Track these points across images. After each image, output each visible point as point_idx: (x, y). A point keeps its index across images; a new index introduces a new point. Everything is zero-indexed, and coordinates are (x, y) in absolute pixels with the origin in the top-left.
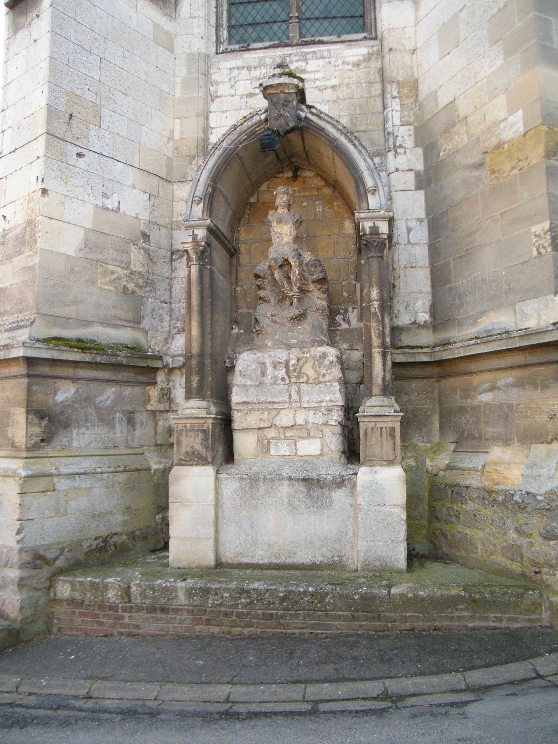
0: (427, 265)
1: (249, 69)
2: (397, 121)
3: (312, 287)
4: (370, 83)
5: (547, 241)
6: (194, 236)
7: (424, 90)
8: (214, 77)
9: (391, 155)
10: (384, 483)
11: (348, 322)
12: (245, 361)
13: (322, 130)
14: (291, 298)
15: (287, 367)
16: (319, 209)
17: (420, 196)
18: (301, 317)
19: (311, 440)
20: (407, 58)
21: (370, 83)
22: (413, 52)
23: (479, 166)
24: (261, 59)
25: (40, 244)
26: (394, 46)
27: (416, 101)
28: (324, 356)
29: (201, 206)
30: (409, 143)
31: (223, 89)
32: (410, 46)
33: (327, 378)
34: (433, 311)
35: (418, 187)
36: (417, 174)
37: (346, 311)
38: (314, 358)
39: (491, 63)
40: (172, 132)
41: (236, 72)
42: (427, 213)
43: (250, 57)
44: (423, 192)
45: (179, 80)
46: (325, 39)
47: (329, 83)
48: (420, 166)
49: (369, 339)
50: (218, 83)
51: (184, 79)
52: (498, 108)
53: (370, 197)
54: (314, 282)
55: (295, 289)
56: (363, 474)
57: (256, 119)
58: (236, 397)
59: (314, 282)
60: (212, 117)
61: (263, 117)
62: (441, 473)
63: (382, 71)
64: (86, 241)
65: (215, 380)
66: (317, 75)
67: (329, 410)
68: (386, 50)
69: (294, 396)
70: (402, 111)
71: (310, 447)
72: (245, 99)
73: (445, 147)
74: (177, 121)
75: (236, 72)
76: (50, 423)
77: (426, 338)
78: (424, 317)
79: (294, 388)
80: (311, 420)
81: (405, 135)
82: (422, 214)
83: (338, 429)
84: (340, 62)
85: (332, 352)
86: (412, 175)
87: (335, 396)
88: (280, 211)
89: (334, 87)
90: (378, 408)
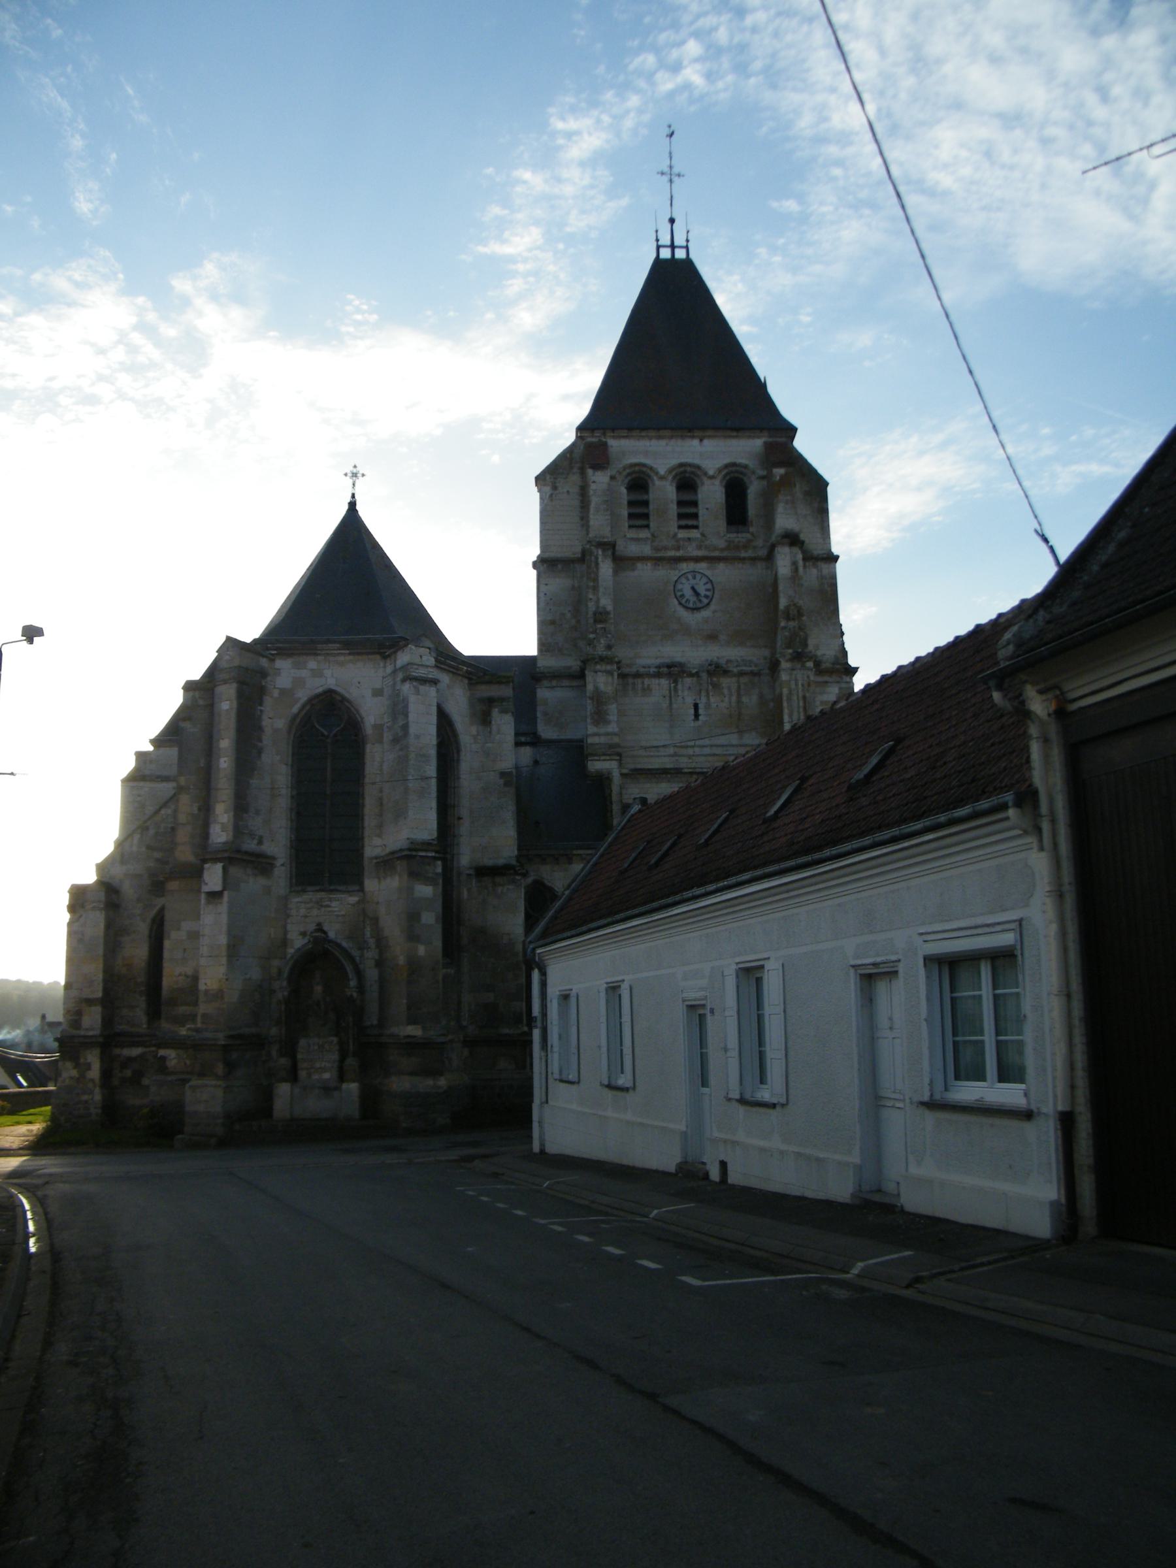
12: (303, 1042)
30: (373, 946)
43: (306, 897)
58: (299, 1056)
65: (289, 1049)
71: (327, 1076)
76: (230, 1066)
85: (335, 1039)
87: (335, 1056)
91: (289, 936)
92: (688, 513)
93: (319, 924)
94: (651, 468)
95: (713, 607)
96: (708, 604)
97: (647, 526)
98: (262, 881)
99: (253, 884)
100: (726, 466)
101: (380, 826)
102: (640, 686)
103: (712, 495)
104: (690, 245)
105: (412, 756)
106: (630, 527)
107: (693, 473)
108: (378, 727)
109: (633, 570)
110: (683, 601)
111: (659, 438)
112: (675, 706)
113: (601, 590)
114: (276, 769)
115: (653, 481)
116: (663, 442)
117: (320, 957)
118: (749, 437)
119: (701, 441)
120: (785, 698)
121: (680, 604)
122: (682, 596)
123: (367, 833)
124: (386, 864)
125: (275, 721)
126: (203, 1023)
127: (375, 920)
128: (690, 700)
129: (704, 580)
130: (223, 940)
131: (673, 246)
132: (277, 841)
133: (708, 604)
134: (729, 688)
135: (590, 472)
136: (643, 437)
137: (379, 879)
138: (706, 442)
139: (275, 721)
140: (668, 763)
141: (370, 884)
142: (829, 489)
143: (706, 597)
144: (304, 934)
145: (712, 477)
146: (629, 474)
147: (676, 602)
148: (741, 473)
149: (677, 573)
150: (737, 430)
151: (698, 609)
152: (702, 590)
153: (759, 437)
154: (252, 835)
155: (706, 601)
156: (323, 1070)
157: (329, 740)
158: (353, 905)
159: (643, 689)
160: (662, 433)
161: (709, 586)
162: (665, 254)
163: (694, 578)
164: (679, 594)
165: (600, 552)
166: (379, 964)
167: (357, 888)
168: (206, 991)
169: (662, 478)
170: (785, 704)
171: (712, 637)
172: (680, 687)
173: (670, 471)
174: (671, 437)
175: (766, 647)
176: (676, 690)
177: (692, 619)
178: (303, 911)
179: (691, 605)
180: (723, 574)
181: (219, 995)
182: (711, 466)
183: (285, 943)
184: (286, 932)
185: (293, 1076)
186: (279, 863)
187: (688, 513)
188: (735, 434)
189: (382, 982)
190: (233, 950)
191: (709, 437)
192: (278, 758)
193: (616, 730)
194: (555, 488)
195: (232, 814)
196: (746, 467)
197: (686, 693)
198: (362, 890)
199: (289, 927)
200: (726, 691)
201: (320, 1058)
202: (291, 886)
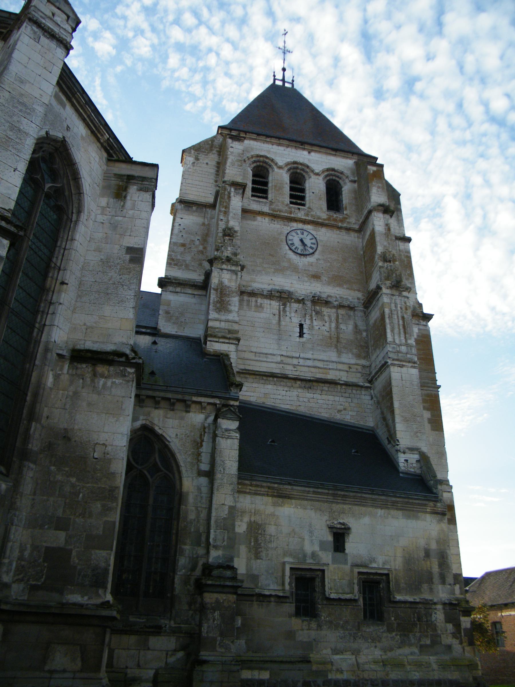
92: (298, 193)
94: (272, 160)
95: (316, 255)
96: (313, 253)
97: (266, 198)
100: (328, 170)
102: (253, 304)
103: (315, 187)
104: (294, 83)
106: (252, 196)
107: (303, 170)
109: (254, 220)
110: (293, 248)
111: (279, 145)
112: (283, 323)
113: (231, 215)
115: (273, 168)
116: (281, 148)
118: (344, 157)
119: (309, 153)
120: (387, 316)
121: (291, 249)
122: (293, 244)
128: (296, 321)
129: (310, 237)
131: (283, 80)
133: (313, 253)
134: (329, 316)
135: (229, 141)
136: (268, 142)
138: (313, 154)
140: (276, 369)
142: (401, 197)
143: (311, 248)
145: (317, 174)
146: (255, 162)
147: (287, 248)
148: (338, 177)
149: (289, 229)
150: (336, 150)
151: (305, 255)
152: (308, 242)
153: (351, 159)
155: (311, 251)
159: (256, 306)
160: (281, 141)
161: (314, 241)
162: (279, 83)
163: (303, 234)
164: (290, 242)
165: (233, 190)
169: (280, 168)
170: (387, 321)
171: (316, 277)
172: (288, 309)
173: (287, 164)
174: (288, 146)
175: (359, 291)
176: (284, 309)
177: (301, 262)
179: (299, 252)
180: (324, 235)
182: (318, 168)
187: (298, 193)
188: (334, 153)
191: (316, 151)
193: (237, 319)
194: (197, 159)
196: (342, 173)
197: (293, 314)
200: (326, 318)
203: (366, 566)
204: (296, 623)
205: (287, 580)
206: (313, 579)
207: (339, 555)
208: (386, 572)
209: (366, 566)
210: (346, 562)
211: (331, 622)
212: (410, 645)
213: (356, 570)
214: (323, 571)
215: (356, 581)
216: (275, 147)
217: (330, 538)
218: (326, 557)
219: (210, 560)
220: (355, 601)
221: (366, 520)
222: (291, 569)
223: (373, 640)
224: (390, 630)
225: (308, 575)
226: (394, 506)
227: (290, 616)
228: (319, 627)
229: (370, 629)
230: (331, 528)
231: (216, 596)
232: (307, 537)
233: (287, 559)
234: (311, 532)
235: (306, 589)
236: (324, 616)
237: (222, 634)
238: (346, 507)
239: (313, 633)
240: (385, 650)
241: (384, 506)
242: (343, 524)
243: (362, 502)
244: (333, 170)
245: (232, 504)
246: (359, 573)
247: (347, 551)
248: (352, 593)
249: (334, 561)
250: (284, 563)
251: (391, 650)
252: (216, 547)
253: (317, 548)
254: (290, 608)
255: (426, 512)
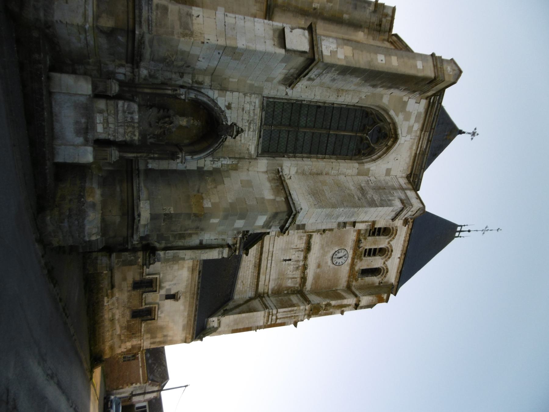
0: (169, 168)
1: (254, 110)
2: (223, 162)
3: (162, 130)
4: (240, 154)
5: (167, 212)
6: (182, 95)
7: (233, 173)
8: (253, 95)
9: (211, 159)
10: (87, 156)
11: (150, 138)
13: (217, 142)
14: (158, 123)
15: (131, 122)
16: (194, 131)
17: (195, 168)
18: (150, 125)
19: (102, 129)
20: (247, 168)
21: (240, 154)
22: (248, 170)
23: (198, 191)
24: (257, 115)
25: (182, 39)
26: (251, 164)
27: (230, 169)
28: (135, 135)
29: (194, 97)
30: (214, 166)
31: (248, 99)
32: (250, 169)
33: (127, 136)
34: (152, 170)
35: (198, 167)
36: (203, 168)
37: (154, 138)
38: (134, 132)
39: (230, 198)
40: (233, 78)
41: (253, 104)
42: (188, 170)
43: (258, 111)
44: (196, 169)
45: (253, 82)
46: (261, 139)
47: (243, 138)
48: (205, 169)
49: (140, 153)
50: (250, 97)
51: (253, 85)
52: (215, 199)
53: (190, 156)
54: (164, 131)
55: (161, 125)
56: (90, 149)
57: (224, 120)
59: (164, 131)
60: (237, 93)
61: (224, 123)
62: (90, 171)
63: (244, 158)
64: (185, 51)
66: (246, 135)
67: (114, 136)
68: (250, 161)
69: (120, 124)
70: (227, 164)
71: (100, 128)
72: (242, 107)
73: (209, 179)
74: (237, 80)
75: (253, 104)
77: (142, 167)
78: (150, 166)
79: (122, 124)
80: (111, 129)
81: (218, 165)
82: (188, 168)
83: (107, 138)
84: (250, 144)
86: (203, 166)
88: (192, 121)
89: (241, 141)
90: (115, 154)
91: (228, 93)
93: (242, 131)
98: (280, 77)
99: (280, 71)
101: (303, 173)
105: (356, 210)
108: (366, 173)
114: (355, 94)
117: (212, 129)
123: (300, 162)
124: (280, 182)
125: (387, 98)
126: (157, 6)
127: (235, 168)
130: (241, 43)
132: (306, 91)
137: (266, 172)
139: (387, 98)
141: (263, 164)
144: (229, 107)
154: (319, 75)
156: (106, 122)
157: (365, 135)
158: (248, 149)
166: (201, 173)
167: (260, 152)
168: (190, 15)
178: (247, 107)
181: (188, 31)
183: (223, 89)
184: (232, 91)
185: (98, 95)
186: (289, 91)
189: (185, 175)
190: (232, 52)
192: (363, 97)
195: (344, 63)
198: (259, 155)
199: (236, 94)
201: (118, 121)
202: (268, 98)
203: (158, 309)
204: (130, 280)
205: (151, 276)
206: (152, 286)
207: (164, 298)
208: (156, 318)
209: (158, 309)
210: (160, 300)
211: (131, 296)
212: (121, 331)
213: (157, 306)
214: (156, 291)
215: (151, 306)
216: (403, 239)
217: (172, 292)
218: (163, 292)
219: (159, 252)
220: (142, 306)
221: (182, 308)
222: (157, 278)
223: (123, 315)
224: (128, 321)
225: (154, 285)
226: (189, 320)
227: (134, 278)
228: (129, 291)
229: (128, 313)
230: (177, 293)
231: (141, 256)
232: (172, 283)
233: (161, 275)
234: (175, 284)
235: (147, 285)
236: (134, 293)
237: (123, 261)
238: (188, 299)
239: (126, 289)
240: (118, 320)
241: (189, 315)
242: (179, 298)
243: (190, 306)
244: (387, 272)
245: (186, 259)
246: (155, 307)
247: (166, 301)
248: (146, 304)
249: (161, 296)
250: (159, 274)
251: (119, 322)
252: (165, 254)
253: (168, 287)
254: (138, 278)
255: (186, 334)
